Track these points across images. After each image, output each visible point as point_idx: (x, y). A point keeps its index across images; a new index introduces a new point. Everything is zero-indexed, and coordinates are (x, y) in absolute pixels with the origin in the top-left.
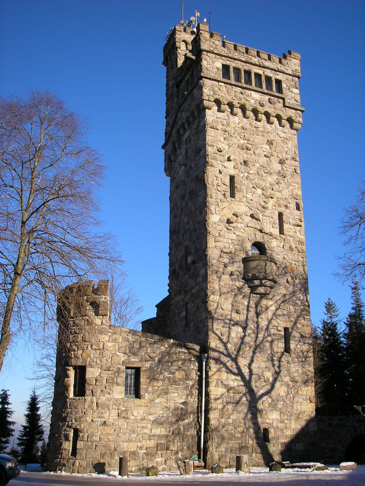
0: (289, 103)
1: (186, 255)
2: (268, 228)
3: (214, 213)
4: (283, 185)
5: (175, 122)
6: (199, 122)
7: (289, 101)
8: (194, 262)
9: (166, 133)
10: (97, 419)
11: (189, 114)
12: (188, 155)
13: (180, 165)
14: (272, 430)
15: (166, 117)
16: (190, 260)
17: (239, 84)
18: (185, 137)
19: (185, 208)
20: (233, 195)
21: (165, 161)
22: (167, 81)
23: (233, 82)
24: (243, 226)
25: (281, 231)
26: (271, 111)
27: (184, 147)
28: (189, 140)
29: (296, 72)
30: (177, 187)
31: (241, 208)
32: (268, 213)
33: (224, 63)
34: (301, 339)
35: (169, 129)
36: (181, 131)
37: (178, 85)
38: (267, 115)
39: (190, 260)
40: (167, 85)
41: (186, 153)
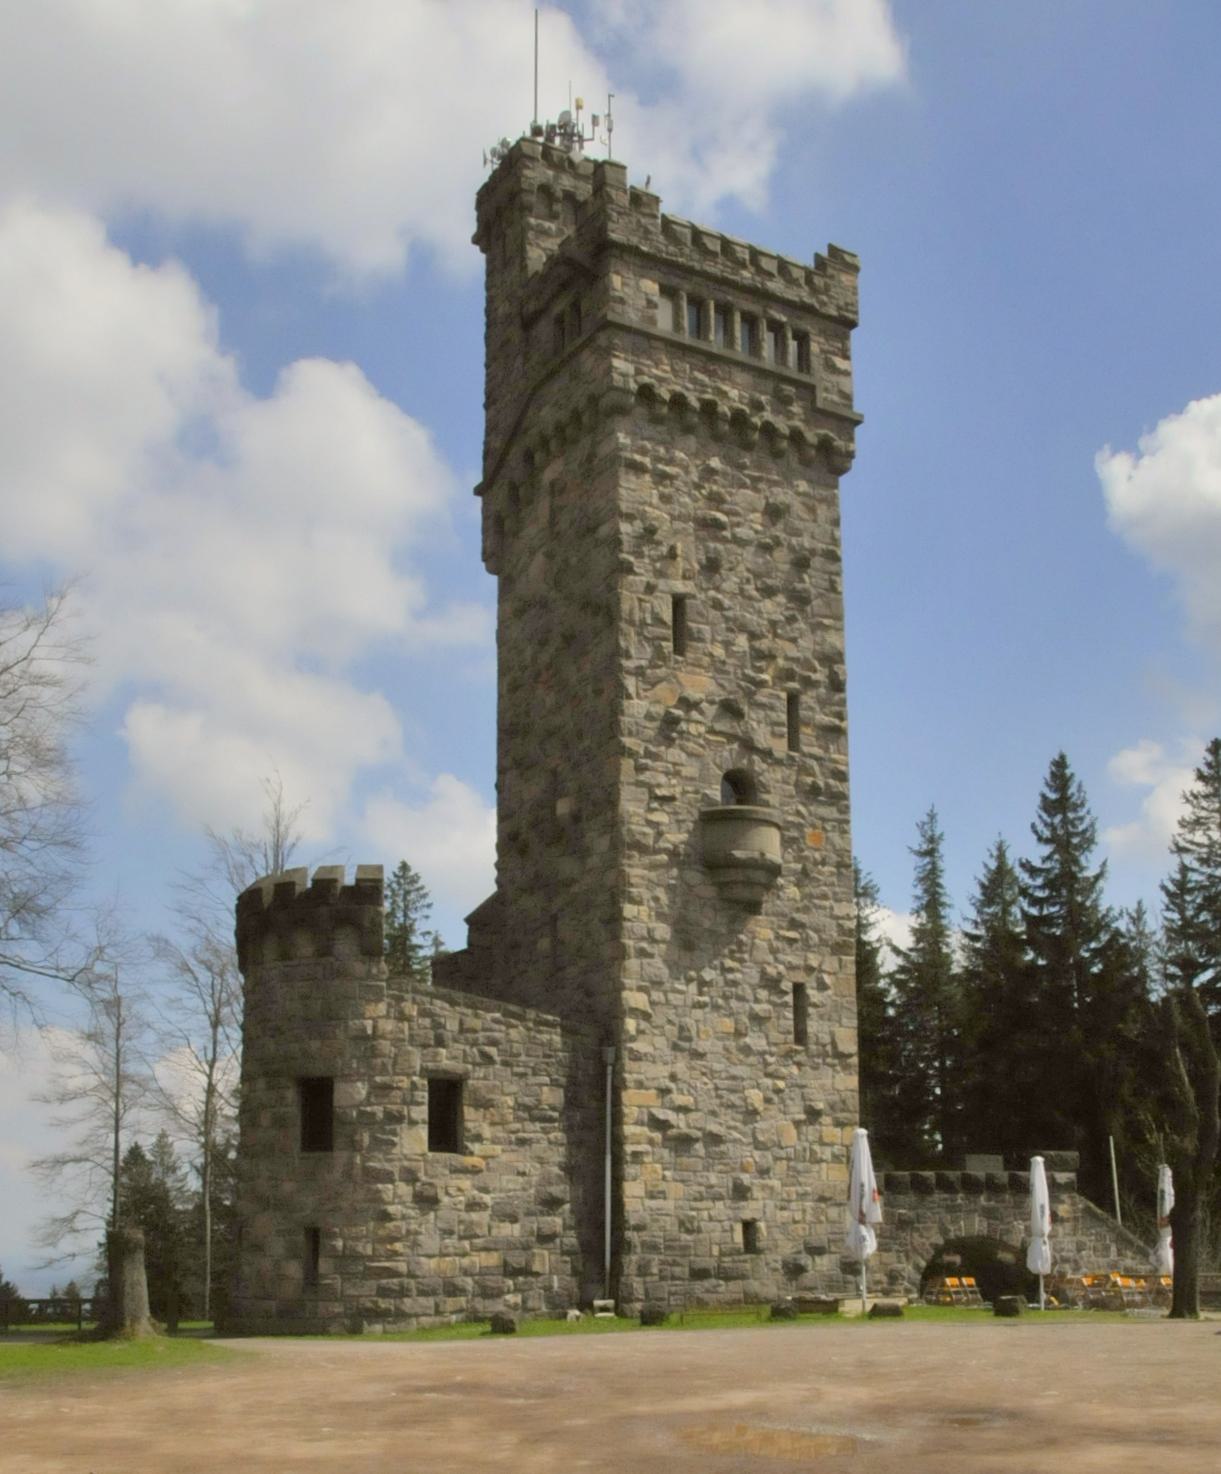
0: (825, 399)
1: (555, 791)
2: (762, 737)
3: (634, 695)
4: (801, 625)
5: (516, 431)
6: (595, 444)
7: (825, 395)
8: (576, 818)
9: (487, 455)
10: (366, 1205)
11: (563, 415)
12: (556, 529)
13: (533, 553)
14: (762, 1225)
15: (487, 406)
16: (563, 807)
17: (702, 345)
18: (548, 475)
19: (547, 669)
20: (679, 649)
21: (485, 531)
22: (490, 300)
23: (687, 335)
24: (702, 729)
25: (793, 744)
26: (782, 425)
27: (543, 507)
28: (556, 489)
29: (847, 311)
30: (519, 613)
31: (700, 685)
32: (762, 697)
33: (665, 282)
34: (534, 1003)
35: (497, 444)
36: (538, 457)
37: (528, 323)
38: (768, 430)
39: (563, 807)
40: (489, 312)
41: (553, 522)
